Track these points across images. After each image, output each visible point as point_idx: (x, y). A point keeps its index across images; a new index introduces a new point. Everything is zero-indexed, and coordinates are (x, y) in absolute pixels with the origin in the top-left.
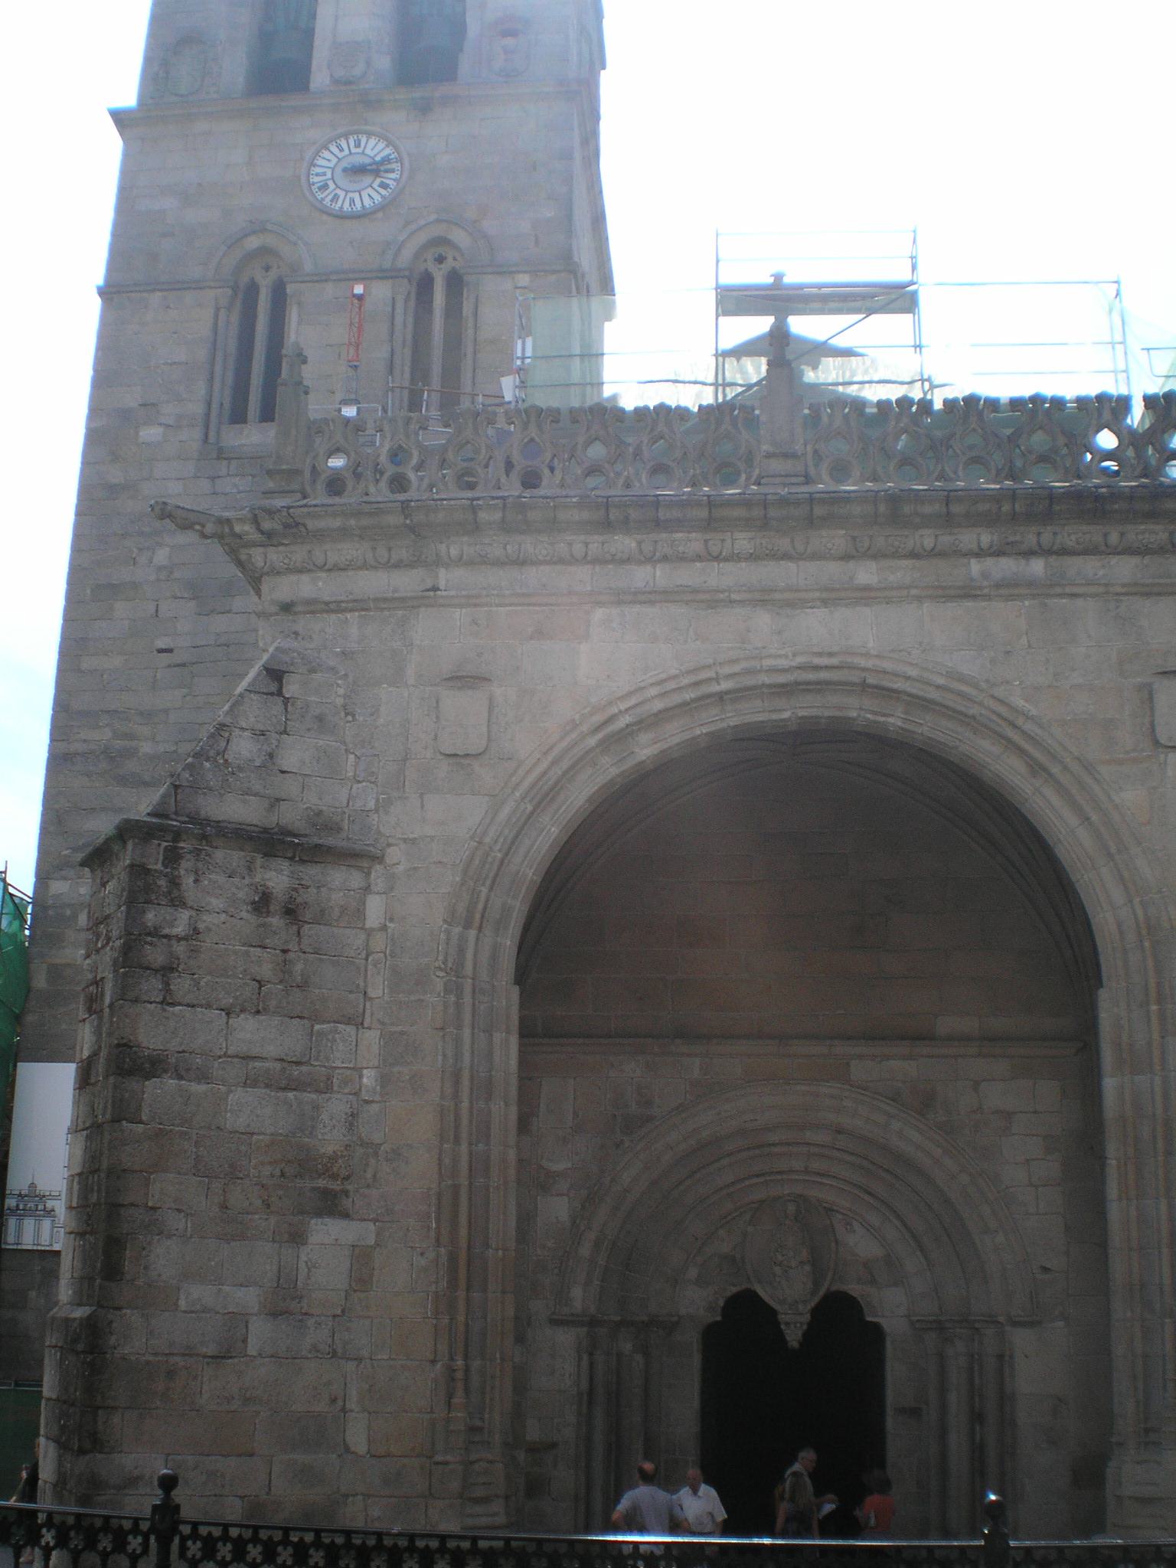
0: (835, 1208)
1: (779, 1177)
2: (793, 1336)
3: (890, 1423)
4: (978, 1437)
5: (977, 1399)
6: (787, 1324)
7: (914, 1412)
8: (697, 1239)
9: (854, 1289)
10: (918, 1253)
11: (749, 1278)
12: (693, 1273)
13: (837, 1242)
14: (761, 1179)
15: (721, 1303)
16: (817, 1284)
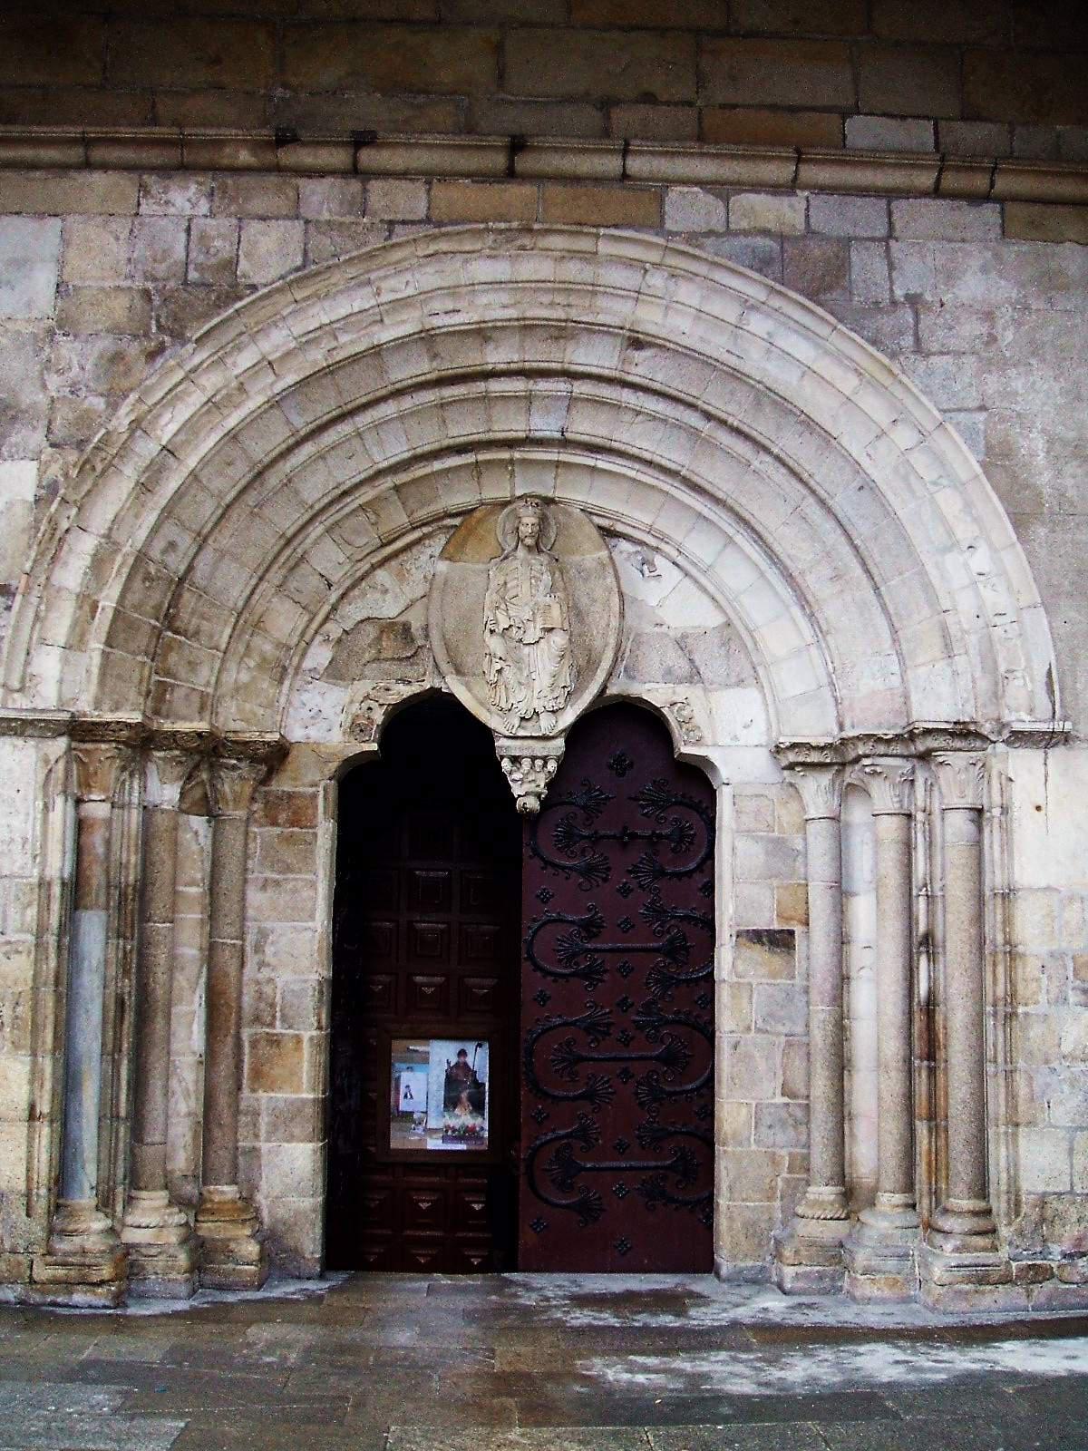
0: (620, 528)
1: (505, 455)
2: (527, 787)
3: (726, 958)
4: (922, 988)
5: (921, 905)
6: (515, 760)
7: (780, 941)
8: (330, 585)
9: (656, 693)
10: (796, 611)
11: (437, 666)
12: (320, 656)
13: (621, 594)
14: (469, 458)
15: (379, 716)
16: (582, 674)
